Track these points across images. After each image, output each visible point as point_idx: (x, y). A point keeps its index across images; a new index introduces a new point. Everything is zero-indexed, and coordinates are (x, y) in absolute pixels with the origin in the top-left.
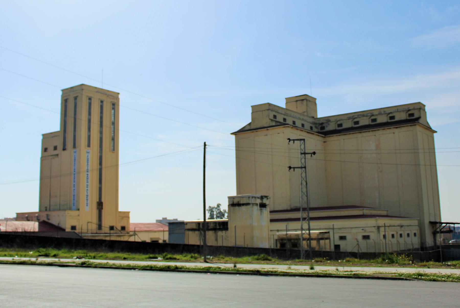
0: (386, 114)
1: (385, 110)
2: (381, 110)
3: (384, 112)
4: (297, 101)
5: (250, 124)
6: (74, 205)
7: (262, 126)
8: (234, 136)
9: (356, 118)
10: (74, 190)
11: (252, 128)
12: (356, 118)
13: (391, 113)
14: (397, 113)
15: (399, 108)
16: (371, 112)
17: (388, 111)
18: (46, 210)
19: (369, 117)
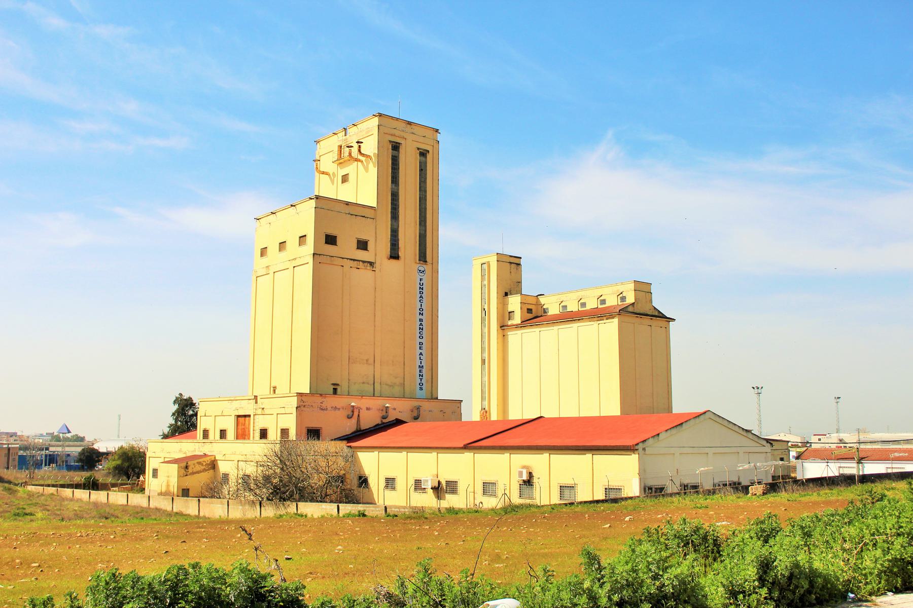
4: (511, 263)
5: (633, 304)
6: (421, 389)
7: (646, 313)
8: (543, 304)
10: (421, 354)
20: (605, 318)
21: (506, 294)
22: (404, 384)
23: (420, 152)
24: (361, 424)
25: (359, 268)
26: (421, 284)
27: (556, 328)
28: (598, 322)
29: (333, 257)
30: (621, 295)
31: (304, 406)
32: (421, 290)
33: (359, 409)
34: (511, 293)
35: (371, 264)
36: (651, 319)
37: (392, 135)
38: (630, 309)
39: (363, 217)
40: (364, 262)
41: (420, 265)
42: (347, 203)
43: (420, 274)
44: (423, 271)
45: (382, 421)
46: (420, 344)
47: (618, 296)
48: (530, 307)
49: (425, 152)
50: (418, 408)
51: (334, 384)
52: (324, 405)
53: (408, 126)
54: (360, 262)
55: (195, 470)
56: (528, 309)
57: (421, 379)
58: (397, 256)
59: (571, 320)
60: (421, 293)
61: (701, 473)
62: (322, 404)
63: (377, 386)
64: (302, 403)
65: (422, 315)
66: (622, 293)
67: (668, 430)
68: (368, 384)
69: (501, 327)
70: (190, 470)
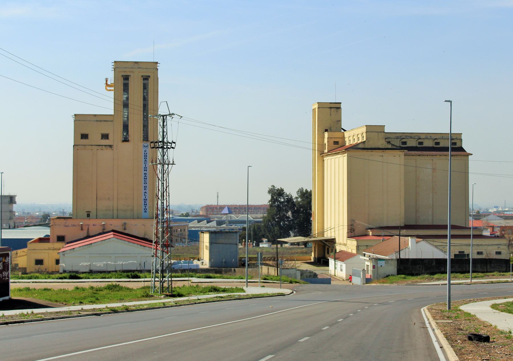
0: (432, 139)
1: (431, 135)
2: (428, 135)
3: (431, 137)
4: (331, 108)
5: (364, 142)
6: (145, 212)
7: (377, 147)
9: (404, 138)
10: (145, 192)
11: (366, 147)
12: (404, 138)
13: (436, 139)
14: (442, 140)
15: (443, 135)
16: (418, 135)
17: (434, 137)
18: (88, 215)
19: (416, 139)
22: (133, 210)
23: (143, 78)
24: (90, 233)
25: (103, 150)
26: (146, 154)
29: (86, 145)
31: (55, 225)
32: (145, 157)
33: (88, 225)
34: (331, 130)
35: (111, 146)
36: (383, 151)
37: (124, 72)
38: (361, 146)
39: (105, 121)
40: (105, 146)
41: (144, 143)
42: (95, 115)
43: (145, 148)
44: (147, 146)
45: (103, 231)
46: (145, 187)
48: (336, 140)
49: (147, 77)
50: (125, 224)
51: (87, 212)
52: (67, 224)
53: (136, 64)
54: (104, 146)
55: (21, 255)
57: (145, 207)
58: (128, 140)
59: (330, 154)
60: (146, 158)
61: (82, 266)
62: (65, 224)
63: (115, 212)
64: (54, 224)
65: (146, 171)
67: (81, 246)
68: (109, 210)
69: (321, 154)
70: (19, 255)
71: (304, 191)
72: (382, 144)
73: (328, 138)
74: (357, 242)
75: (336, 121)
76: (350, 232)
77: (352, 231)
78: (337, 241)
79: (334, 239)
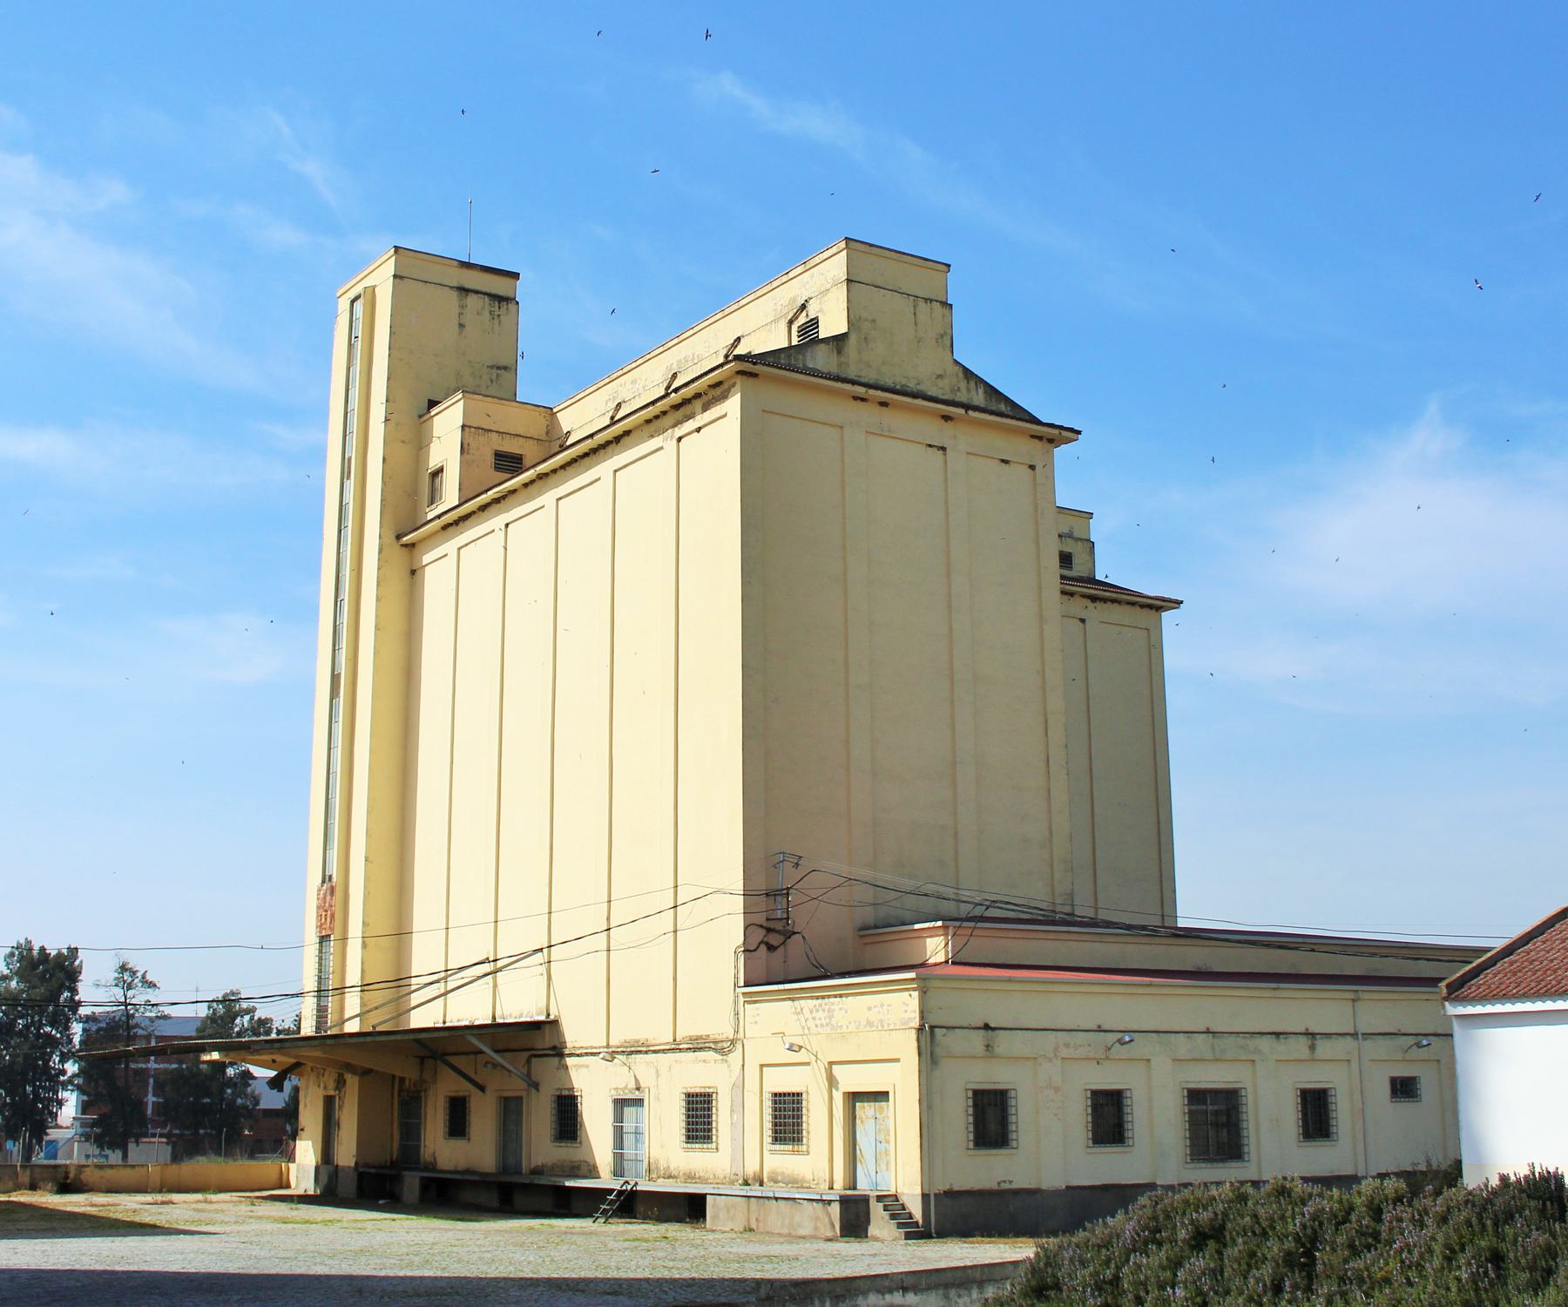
4: (463, 290)
7: (912, 385)
11: (852, 373)
20: (698, 404)
21: (432, 404)
27: (548, 498)
28: (679, 432)
30: (802, 320)
47: (791, 322)
56: (499, 456)
66: (803, 307)
69: (399, 537)
71: (35, 953)
72: (940, 376)
73: (463, 427)
74: (924, 992)
75: (492, 367)
76: (762, 942)
77: (774, 940)
78: (573, 1035)
79: (549, 1026)
